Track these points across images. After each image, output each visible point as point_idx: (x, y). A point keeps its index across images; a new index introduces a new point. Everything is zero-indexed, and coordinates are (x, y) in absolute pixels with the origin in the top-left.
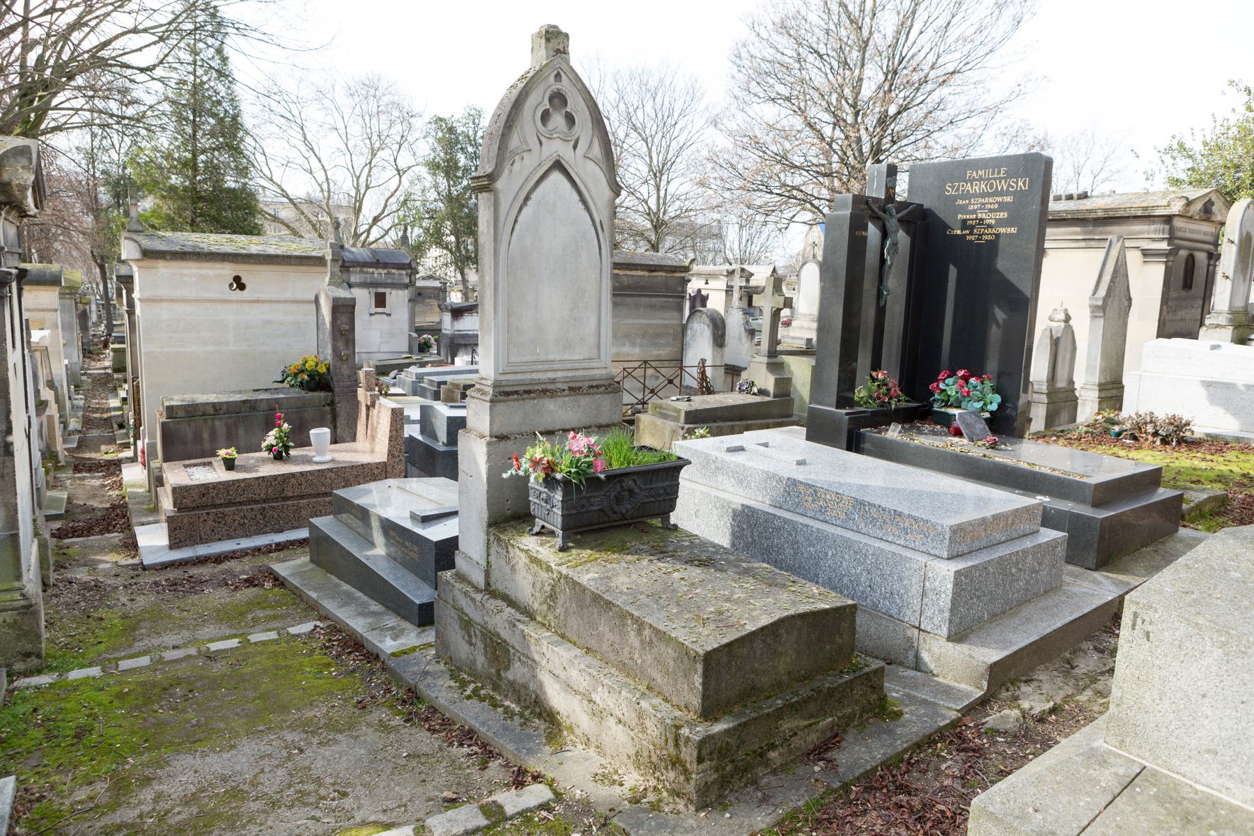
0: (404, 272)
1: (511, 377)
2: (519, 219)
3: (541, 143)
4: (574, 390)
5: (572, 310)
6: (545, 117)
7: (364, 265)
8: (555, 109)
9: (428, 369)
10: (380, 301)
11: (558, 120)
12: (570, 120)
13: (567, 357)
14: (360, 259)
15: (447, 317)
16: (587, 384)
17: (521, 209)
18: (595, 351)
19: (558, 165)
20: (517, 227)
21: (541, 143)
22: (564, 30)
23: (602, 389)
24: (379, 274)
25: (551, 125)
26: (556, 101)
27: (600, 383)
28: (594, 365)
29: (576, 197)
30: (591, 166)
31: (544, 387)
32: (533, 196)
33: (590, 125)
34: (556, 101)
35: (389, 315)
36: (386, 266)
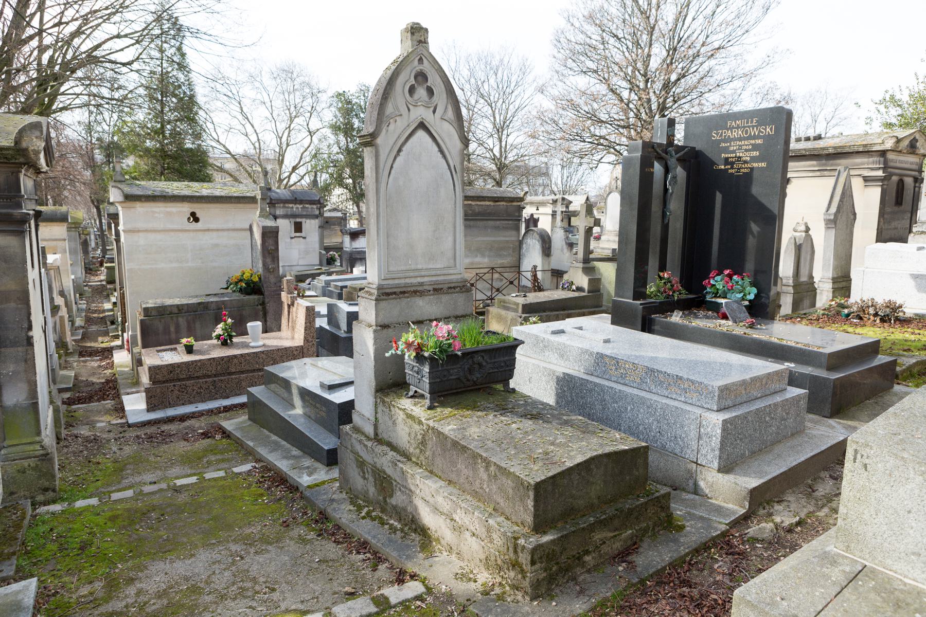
0: (315, 206)
5: (435, 231)
6: (412, 90)
7: (285, 202)
9: (334, 277)
10: (298, 228)
11: (421, 92)
12: (430, 92)
13: (431, 266)
14: (283, 197)
15: (347, 239)
16: (447, 286)
18: (452, 261)
19: (422, 126)
20: (393, 171)
22: (424, 26)
24: (297, 208)
25: (416, 96)
27: (456, 285)
28: (451, 272)
29: (436, 149)
30: (446, 125)
31: (415, 289)
33: (445, 95)
34: (420, 78)
35: (304, 238)
36: (301, 202)
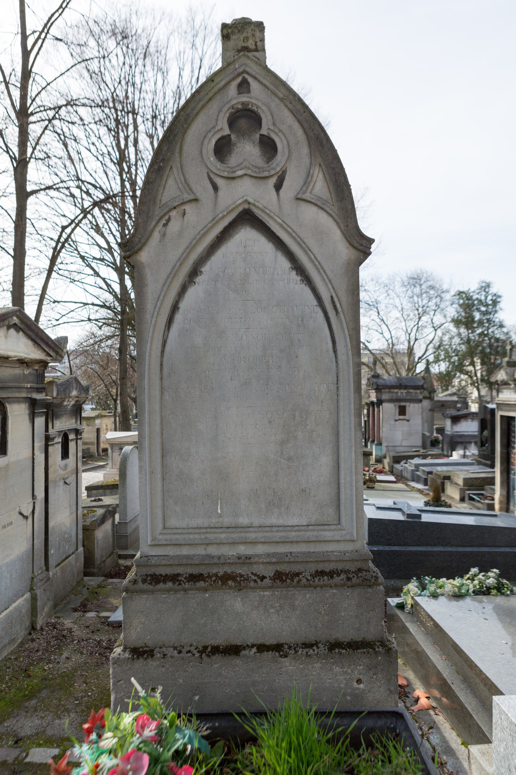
0: (418, 391)
1: (171, 551)
2: (182, 305)
3: (216, 188)
4: (284, 578)
5: (283, 443)
6: (223, 148)
7: (391, 387)
8: (242, 134)
9: (429, 461)
10: (402, 411)
11: (247, 151)
12: (269, 147)
13: (274, 520)
14: (388, 383)
15: (448, 422)
16: (313, 568)
17: (183, 289)
18: (331, 511)
19: (248, 217)
20: (178, 317)
21: (216, 188)
22: (255, 18)
23: (337, 580)
24: (401, 393)
25: (233, 160)
26: (243, 123)
27: (340, 566)
28: (328, 535)
29: (284, 263)
30: (310, 212)
31: (229, 570)
32: (206, 269)
33: (305, 150)
34: (243, 123)
35: (408, 421)
36: (406, 387)
